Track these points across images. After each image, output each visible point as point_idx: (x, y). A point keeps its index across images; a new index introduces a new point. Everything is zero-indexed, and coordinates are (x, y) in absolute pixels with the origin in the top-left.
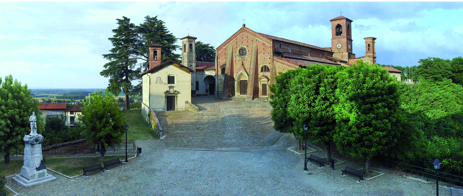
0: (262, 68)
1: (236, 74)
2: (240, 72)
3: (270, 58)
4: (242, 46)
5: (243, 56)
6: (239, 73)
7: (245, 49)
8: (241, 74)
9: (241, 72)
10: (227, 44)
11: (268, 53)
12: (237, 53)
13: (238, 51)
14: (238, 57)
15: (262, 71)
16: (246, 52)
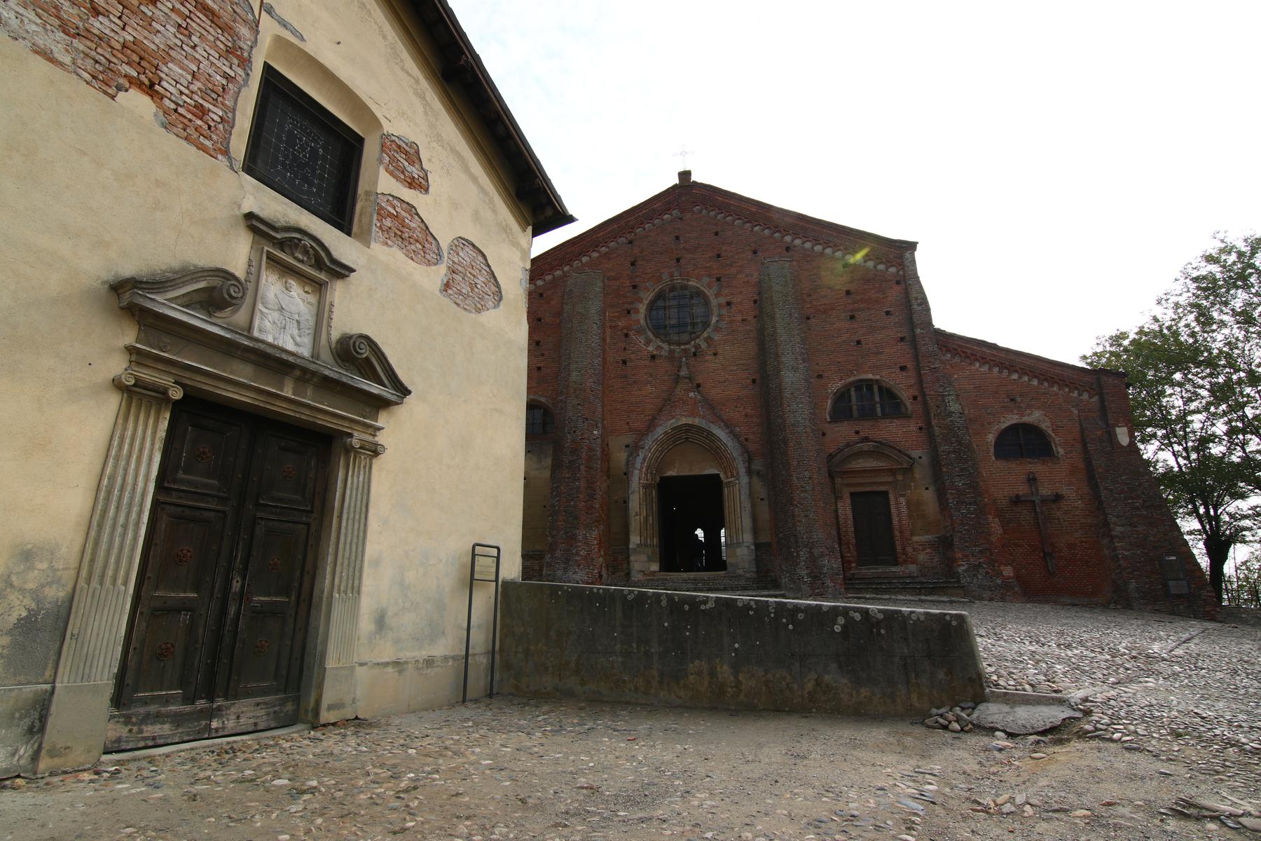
0: (842, 397)
1: (628, 439)
2: (673, 423)
3: (902, 339)
4: (678, 280)
5: (685, 337)
6: (659, 432)
7: (699, 294)
8: (685, 437)
9: (684, 421)
10: (552, 269)
11: (888, 313)
12: (634, 316)
13: (642, 308)
14: (642, 339)
15: (842, 411)
16: (708, 315)
